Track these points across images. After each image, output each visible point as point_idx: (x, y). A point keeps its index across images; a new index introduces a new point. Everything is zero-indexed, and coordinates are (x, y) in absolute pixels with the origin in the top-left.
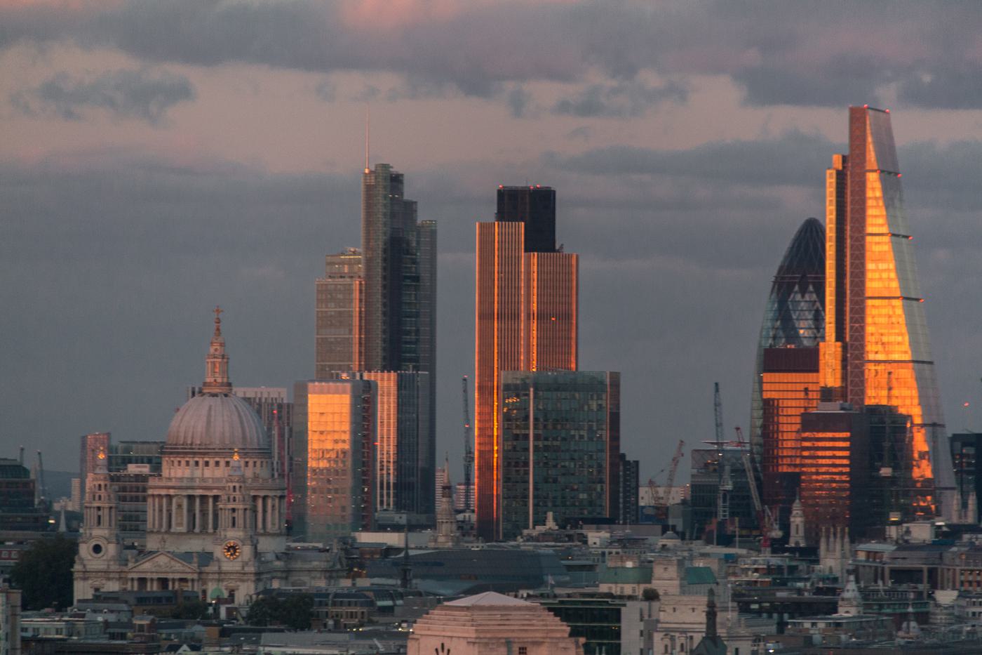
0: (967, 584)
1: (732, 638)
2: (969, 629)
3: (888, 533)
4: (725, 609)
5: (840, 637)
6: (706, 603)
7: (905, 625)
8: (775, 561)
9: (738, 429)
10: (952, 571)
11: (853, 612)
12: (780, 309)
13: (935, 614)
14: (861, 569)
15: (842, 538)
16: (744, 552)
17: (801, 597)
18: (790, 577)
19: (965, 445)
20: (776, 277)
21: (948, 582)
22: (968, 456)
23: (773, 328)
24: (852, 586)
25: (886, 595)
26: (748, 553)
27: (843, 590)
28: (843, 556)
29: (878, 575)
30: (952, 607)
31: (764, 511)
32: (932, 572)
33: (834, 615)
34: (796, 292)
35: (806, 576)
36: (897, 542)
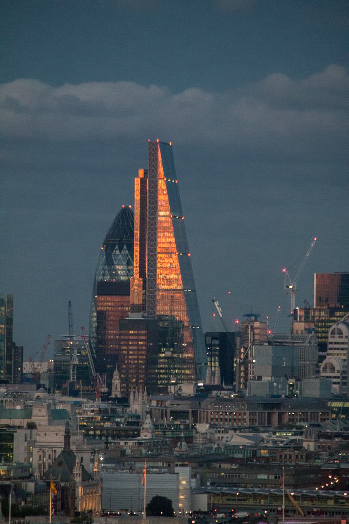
0: (215, 420)
1: (79, 451)
2: (216, 446)
3: (169, 390)
4: (75, 434)
5: (141, 451)
6: (64, 431)
7: (179, 444)
8: (104, 405)
9: (83, 328)
10: (206, 412)
11: (149, 436)
12: (107, 259)
13: (196, 438)
14: (153, 411)
15: (143, 393)
16: (85, 400)
19: (213, 338)
20: (105, 241)
22: (216, 346)
23: (103, 270)
24: (148, 420)
25: (168, 426)
26: (87, 401)
27: (143, 423)
28: (143, 403)
29: (163, 414)
30: (207, 433)
31: (97, 376)
32: (195, 414)
33: (138, 438)
34: (116, 249)
35: (121, 415)
36: (174, 395)
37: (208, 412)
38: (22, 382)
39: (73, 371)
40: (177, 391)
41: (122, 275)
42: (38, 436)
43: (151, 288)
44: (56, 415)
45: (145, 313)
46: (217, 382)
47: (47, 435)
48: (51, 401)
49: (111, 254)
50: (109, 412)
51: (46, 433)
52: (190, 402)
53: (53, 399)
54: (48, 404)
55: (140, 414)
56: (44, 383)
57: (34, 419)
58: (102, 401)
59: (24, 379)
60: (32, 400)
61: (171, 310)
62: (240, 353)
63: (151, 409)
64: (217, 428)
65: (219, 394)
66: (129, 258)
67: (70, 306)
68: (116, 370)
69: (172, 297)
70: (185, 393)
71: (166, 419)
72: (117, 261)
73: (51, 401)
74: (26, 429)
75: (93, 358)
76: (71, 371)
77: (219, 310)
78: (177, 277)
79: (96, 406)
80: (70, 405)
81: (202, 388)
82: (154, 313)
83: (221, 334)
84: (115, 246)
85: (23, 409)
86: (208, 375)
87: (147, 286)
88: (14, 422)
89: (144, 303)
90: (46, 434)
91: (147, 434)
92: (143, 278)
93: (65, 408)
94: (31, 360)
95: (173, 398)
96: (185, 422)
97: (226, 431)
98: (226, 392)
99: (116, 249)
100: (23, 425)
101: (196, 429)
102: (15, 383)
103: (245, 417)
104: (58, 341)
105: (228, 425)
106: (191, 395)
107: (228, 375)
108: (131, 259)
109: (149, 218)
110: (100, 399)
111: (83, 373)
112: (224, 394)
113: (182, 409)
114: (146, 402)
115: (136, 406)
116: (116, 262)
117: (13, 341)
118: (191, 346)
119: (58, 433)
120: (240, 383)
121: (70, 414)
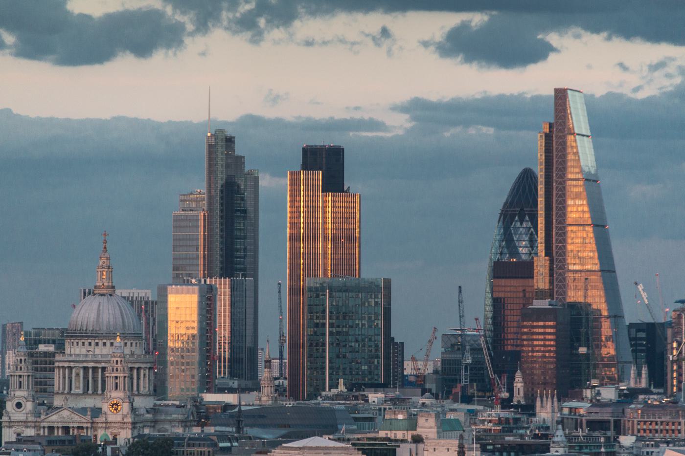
0: (642, 431)
3: (584, 394)
4: (471, 449)
6: (457, 445)
8: (504, 414)
9: (477, 319)
10: (631, 422)
12: (505, 233)
14: (565, 421)
16: (481, 408)
17: (522, 440)
18: (515, 426)
19: (638, 331)
20: (502, 211)
21: (629, 429)
22: (641, 339)
24: (560, 432)
25: (584, 439)
26: (484, 409)
28: (553, 411)
29: (577, 425)
30: (632, 448)
31: (494, 379)
34: (516, 221)
35: (526, 426)
37: (633, 421)
38: (402, 386)
39: (465, 372)
40: (595, 396)
41: (523, 253)
42: (425, 452)
43: (560, 268)
44: (446, 427)
45: (553, 299)
46: (644, 384)
47: (436, 451)
48: (439, 409)
49: (509, 228)
50: (511, 422)
51: (436, 448)
52: (609, 410)
53: (442, 406)
54: (436, 412)
55: (550, 425)
56: (430, 387)
57: (419, 431)
58: (503, 408)
59: (406, 383)
60: (416, 407)
61: (585, 296)
62: (673, 349)
63: (563, 419)
64: (645, 441)
65: (647, 400)
66: (532, 232)
67: (460, 291)
68: (519, 371)
69: (586, 279)
70: (604, 399)
71: (582, 431)
72: (517, 236)
73: (439, 409)
74: (411, 443)
75: (490, 355)
76: (463, 372)
77: (644, 295)
78: (591, 254)
79: (494, 415)
80: (463, 414)
81: (625, 392)
82: (564, 298)
83: (649, 324)
84: (515, 217)
85: (406, 419)
86: (632, 376)
87: (555, 266)
88: (395, 434)
89: (551, 288)
90: (435, 450)
91: (558, 449)
92: (551, 257)
93: (457, 418)
94: (414, 359)
95: (590, 405)
96: (606, 434)
97: (657, 445)
98: (655, 397)
99: (516, 221)
100: (406, 438)
101: (619, 443)
102: (395, 387)
103: (679, 427)
104: (445, 335)
105: (658, 437)
106: (613, 401)
107: (658, 378)
108: (534, 233)
109: (557, 182)
110: (499, 406)
111: (477, 372)
112: (653, 400)
113: (600, 418)
114: (556, 410)
115: (545, 412)
116: (516, 237)
117: (392, 336)
118: (611, 340)
119: (450, 448)
120: (673, 386)
121: (463, 425)
